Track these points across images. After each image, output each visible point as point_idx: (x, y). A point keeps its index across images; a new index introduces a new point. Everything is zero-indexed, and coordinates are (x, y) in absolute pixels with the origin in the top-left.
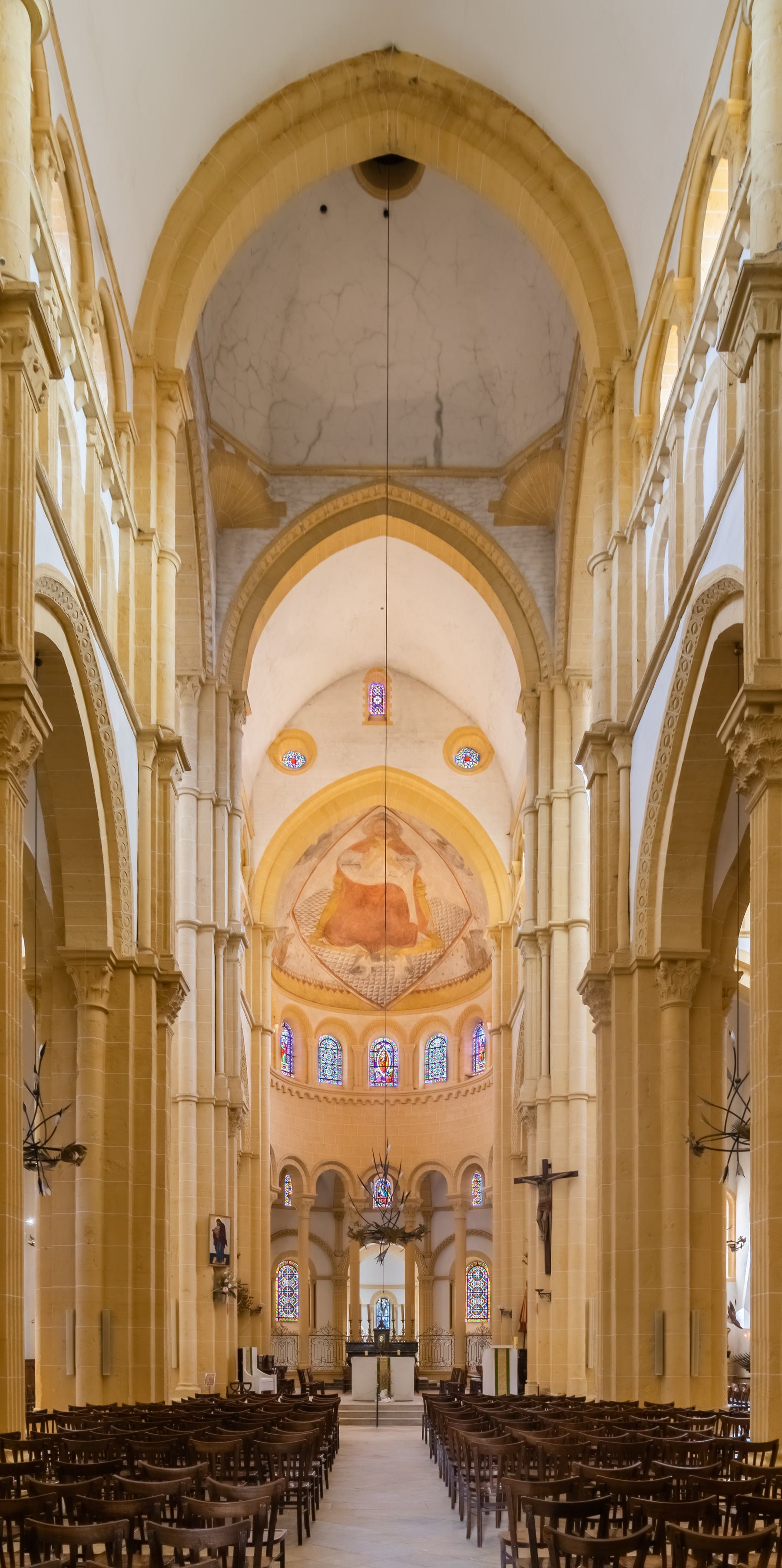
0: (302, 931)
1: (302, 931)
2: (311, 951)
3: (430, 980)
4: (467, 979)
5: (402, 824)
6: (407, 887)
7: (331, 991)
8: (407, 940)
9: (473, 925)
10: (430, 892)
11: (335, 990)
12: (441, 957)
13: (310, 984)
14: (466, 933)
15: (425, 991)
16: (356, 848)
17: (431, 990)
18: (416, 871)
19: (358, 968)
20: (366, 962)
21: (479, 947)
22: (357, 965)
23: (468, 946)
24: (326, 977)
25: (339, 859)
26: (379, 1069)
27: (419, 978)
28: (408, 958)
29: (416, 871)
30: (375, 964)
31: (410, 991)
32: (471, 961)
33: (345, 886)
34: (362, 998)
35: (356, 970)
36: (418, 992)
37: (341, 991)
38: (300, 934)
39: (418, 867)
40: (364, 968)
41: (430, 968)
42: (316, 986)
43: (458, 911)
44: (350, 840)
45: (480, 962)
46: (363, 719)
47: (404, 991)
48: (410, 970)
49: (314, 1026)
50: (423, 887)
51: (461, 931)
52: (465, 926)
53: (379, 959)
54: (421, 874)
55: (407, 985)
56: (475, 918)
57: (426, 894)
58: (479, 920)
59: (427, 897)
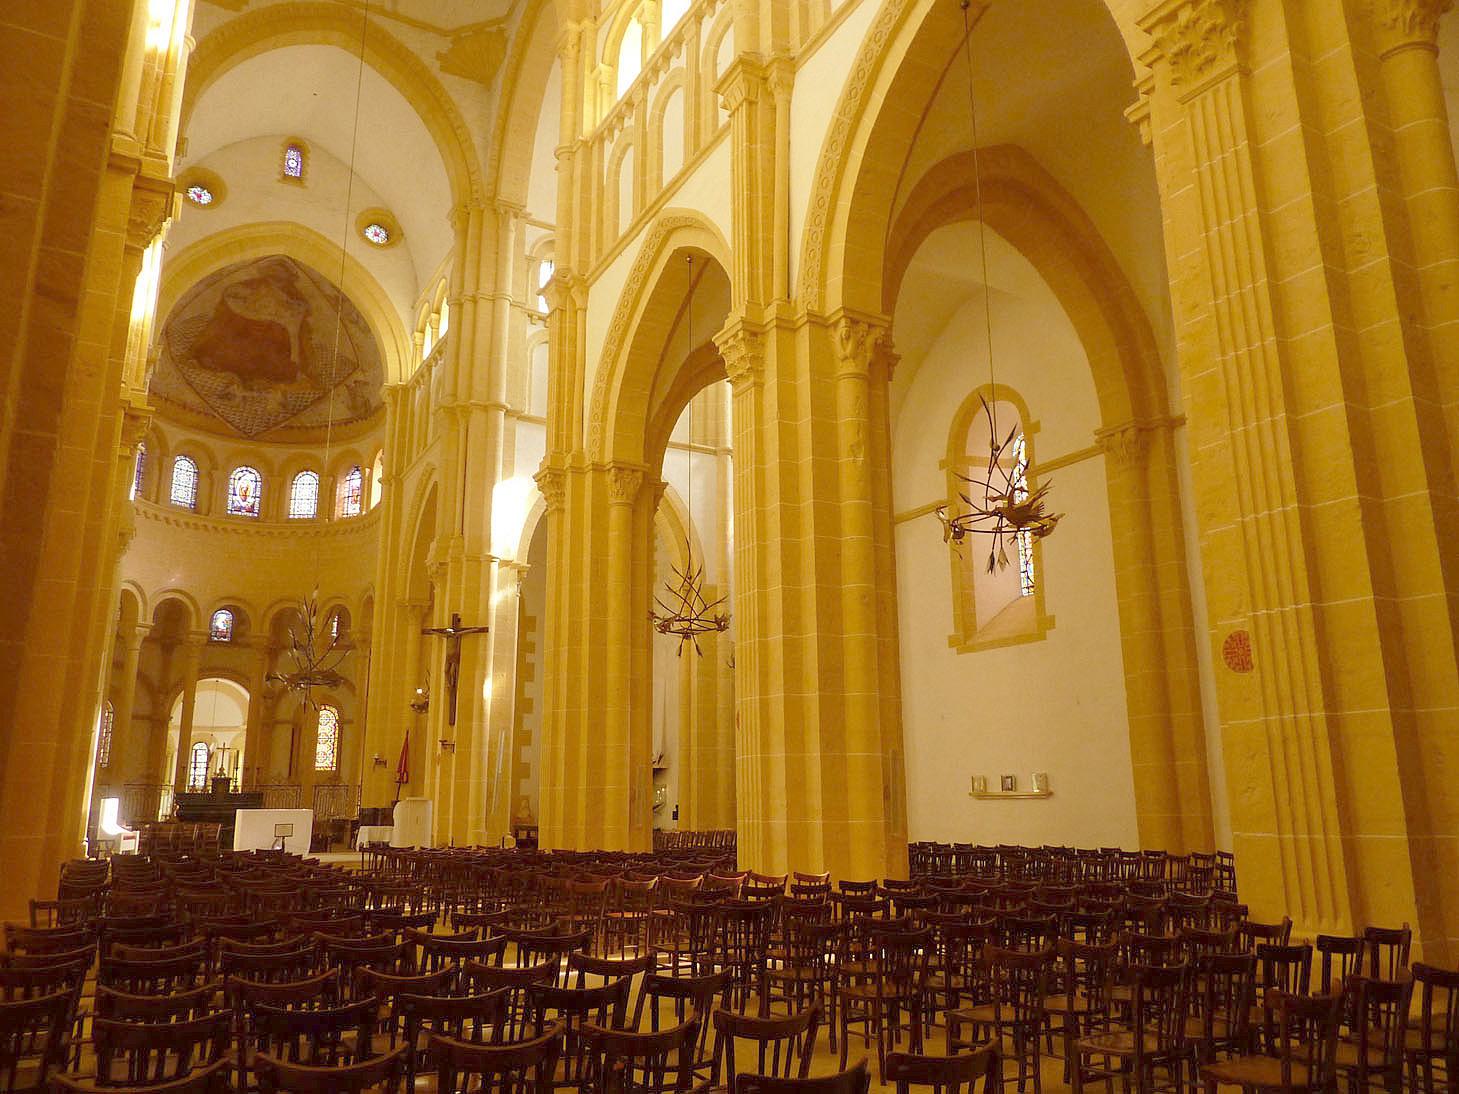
0: (172, 349)
1: (172, 349)
2: (181, 371)
3: (307, 419)
4: (346, 424)
5: (300, 273)
6: (293, 330)
7: (194, 414)
8: (286, 375)
9: (359, 376)
10: (316, 338)
11: (200, 413)
12: (319, 398)
13: (172, 402)
14: (350, 382)
15: (299, 428)
16: (248, 284)
17: (307, 428)
18: (305, 317)
19: (229, 393)
20: (237, 390)
21: (363, 397)
22: (227, 391)
23: (350, 394)
24: (190, 398)
25: (226, 289)
26: (238, 498)
27: (295, 415)
28: (284, 394)
29: (305, 317)
30: (247, 394)
31: (283, 425)
32: (353, 408)
33: (225, 318)
34: (229, 425)
35: (226, 396)
36: (292, 428)
37: (206, 414)
38: (170, 353)
39: (308, 313)
40: (235, 396)
41: (306, 407)
42: (179, 405)
43: (344, 361)
44: (243, 276)
45: (363, 410)
46: (279, 177)
47: (275, 425)
48: (284, 405)
49: (172, 445)
50: (310, 332)
51: (345, 378)
52: (350, 375)
53: (252, 390)
54: (310, 320)
55: (279, 419)
56: (363, 371)
57: (311, 339)
58: (367, 374)
59: (313, 342)
